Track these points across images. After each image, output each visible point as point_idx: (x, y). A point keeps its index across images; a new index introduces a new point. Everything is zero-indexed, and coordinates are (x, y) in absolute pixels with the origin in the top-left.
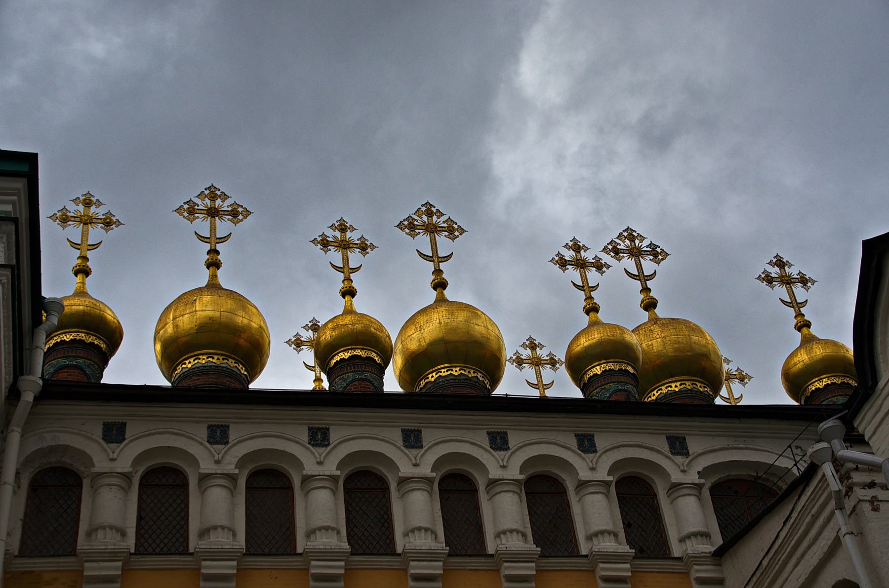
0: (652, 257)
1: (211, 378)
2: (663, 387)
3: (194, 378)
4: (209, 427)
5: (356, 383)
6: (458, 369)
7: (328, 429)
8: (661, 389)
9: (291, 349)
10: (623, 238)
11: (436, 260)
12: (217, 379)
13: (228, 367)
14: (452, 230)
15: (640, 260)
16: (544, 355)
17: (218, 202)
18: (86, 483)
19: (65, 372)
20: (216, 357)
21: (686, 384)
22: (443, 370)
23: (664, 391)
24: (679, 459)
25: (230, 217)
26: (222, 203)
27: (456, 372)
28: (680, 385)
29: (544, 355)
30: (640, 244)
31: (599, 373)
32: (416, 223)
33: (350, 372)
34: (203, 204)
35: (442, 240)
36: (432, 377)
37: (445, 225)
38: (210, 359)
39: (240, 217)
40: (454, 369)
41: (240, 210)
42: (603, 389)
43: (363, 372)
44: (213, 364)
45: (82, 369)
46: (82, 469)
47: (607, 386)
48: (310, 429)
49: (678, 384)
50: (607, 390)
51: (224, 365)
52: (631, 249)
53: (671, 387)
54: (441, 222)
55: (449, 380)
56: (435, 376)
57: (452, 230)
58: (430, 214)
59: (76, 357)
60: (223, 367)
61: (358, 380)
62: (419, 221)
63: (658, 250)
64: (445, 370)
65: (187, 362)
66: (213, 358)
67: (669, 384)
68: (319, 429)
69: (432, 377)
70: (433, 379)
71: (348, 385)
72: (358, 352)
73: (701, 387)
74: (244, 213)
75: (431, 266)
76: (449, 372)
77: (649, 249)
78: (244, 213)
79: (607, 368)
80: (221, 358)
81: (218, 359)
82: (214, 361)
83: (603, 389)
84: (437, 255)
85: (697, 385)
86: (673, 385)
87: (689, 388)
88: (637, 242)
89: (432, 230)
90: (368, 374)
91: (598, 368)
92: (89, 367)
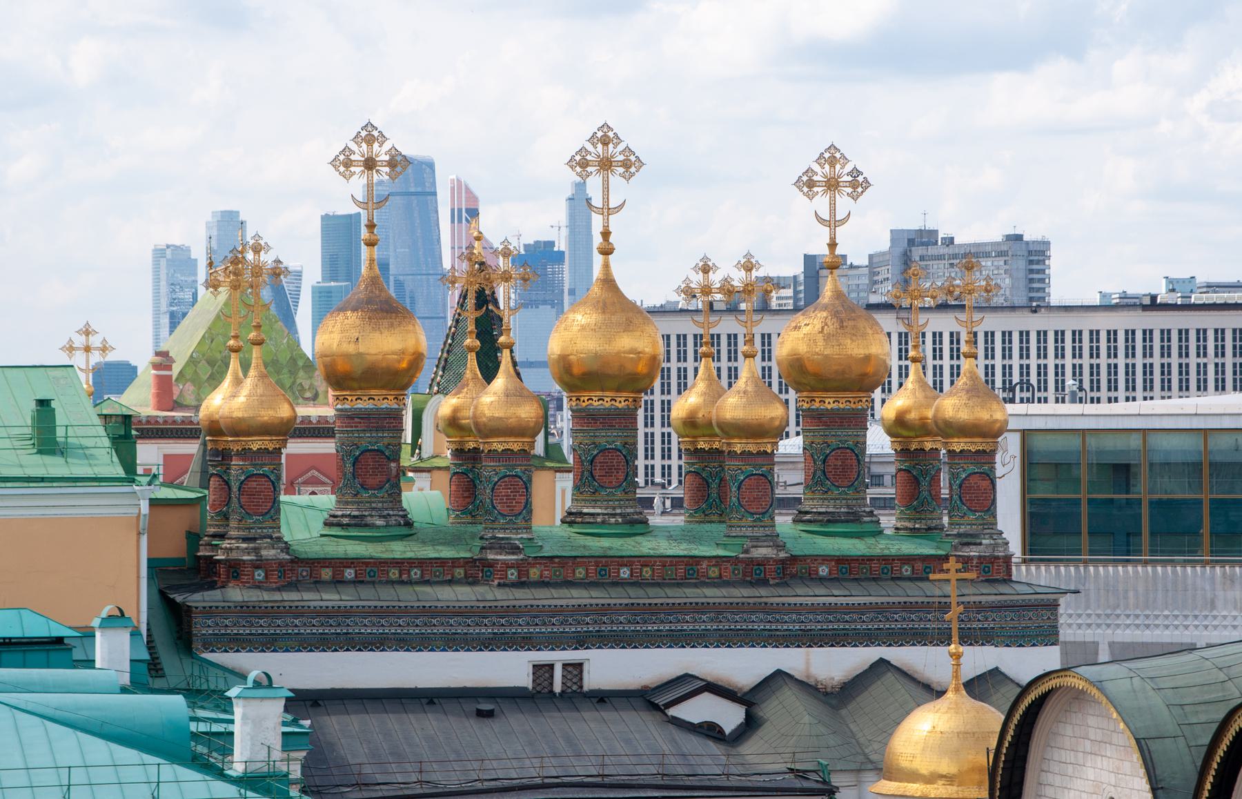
0: (849, 190)
1: (372, 423)
2: (817, 400)
3: (356, 420)
5: (506, 479)
6: (609, 399)
8: (814, 401)
10: (823, 161)
11: (606, 213)
14: (630, 165)
15: (835, 197)
16: (717, 281)
17: (376, 145)
19: (254, 481)
20: (376, 398)
22: (594, 399)
28: (834, 402)
29: (717, 281)
30: (841, 171)
31: (739, 452)
32: (589, 157)
33: (503, 466)
34: (359, 152)
35: (616, 180)
36: (584, 401)
37: (621, 158)
38: (371, 401)
40: (606, 399)
42: (740, 469)
43: (514, 467)
45: (268, 477)
47: (743, 468)
49: (831, 401)
51: (384, 406)
52: (829, 180)
53: (824, 402)
54: (617, 154)
55: (600, 409)
56: (587, 403)
58: (605, 141)
59: (262, 466)
61: (509, 476)
62: (593, 155)
63: (860, 179)
64: (596, 399)
65: (350, 398)
66: (374, 399)
69: (584, 401)
70: (584, 404)
71: (499, 480)
73: (854, 403)
76: (601, 402)
77: (850, 179)
79: (747, 450)
80: (381, 398)
83: (740, 469)
84: (608, 205)
85: (850, 402)
91: (739, 445)
92: (272, 472)
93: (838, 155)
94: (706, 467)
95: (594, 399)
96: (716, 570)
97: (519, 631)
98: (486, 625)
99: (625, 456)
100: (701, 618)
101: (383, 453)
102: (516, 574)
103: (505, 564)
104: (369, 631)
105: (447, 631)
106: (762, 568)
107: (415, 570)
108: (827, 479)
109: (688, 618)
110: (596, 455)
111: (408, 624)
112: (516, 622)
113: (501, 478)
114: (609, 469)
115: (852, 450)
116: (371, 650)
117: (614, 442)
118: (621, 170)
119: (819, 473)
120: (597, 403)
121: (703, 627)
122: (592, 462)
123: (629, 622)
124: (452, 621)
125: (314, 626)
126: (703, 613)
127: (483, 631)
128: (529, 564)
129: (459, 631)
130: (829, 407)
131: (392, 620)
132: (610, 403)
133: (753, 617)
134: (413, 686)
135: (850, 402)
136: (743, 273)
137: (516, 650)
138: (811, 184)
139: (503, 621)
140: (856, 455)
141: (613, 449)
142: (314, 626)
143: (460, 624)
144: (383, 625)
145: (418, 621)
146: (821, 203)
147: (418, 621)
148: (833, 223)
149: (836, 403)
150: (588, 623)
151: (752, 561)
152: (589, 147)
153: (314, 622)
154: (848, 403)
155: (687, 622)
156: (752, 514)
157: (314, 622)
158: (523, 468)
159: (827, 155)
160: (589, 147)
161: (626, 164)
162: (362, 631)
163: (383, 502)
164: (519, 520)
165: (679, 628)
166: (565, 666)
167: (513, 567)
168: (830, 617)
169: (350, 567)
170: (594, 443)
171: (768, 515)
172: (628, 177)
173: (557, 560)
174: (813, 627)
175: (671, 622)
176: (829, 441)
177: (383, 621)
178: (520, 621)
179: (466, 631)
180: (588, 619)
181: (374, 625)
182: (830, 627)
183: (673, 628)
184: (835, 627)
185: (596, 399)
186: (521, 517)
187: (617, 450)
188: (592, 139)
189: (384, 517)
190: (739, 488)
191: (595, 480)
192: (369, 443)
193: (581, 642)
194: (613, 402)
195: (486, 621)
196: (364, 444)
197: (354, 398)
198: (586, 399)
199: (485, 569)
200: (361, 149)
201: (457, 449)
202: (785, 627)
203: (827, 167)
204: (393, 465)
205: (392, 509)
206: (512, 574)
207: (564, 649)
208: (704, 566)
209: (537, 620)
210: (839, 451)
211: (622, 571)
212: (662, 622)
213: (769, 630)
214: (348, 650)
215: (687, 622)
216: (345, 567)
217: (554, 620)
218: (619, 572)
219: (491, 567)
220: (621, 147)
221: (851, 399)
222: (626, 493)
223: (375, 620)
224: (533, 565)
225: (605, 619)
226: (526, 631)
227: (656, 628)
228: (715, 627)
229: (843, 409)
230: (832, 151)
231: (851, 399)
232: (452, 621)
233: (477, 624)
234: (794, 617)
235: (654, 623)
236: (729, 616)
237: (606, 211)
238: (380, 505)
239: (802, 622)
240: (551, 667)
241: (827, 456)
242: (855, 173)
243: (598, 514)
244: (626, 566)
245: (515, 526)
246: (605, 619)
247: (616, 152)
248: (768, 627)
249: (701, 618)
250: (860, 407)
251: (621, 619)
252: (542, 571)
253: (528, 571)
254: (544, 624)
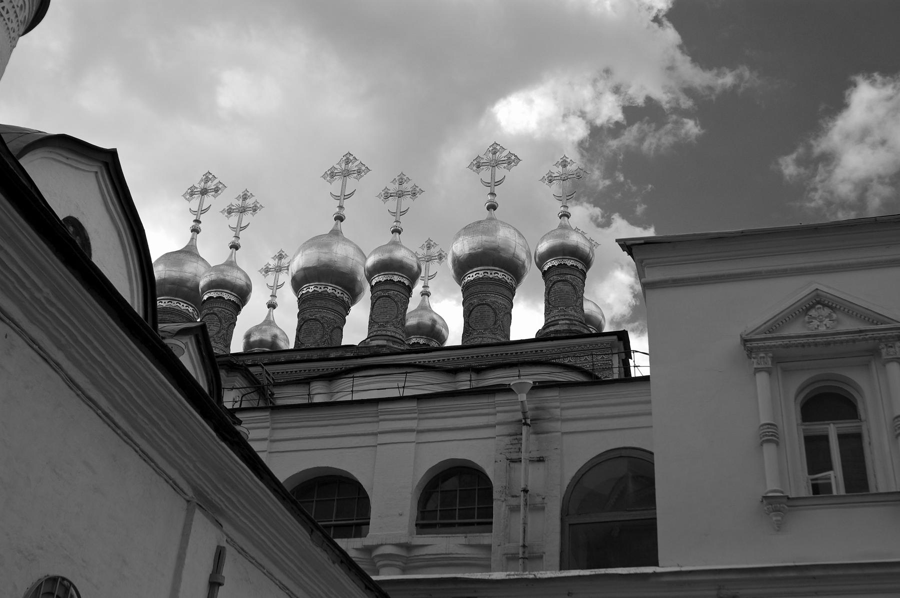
9: (261, 276)
12: (162, 316)
13: (172, 307)
44: (161, 307)
51: (168, 306)
60: (167, 308)
67: (477, 272)
81: (165, 303)
85: (488, 273)
90: (216, 309)
99: (321, 323)
108: (470, 327)
110: (303, 325)
114: (311, 332)
132: (313, 290)
135: (488, 273)
149: (478, 275)
154: (486, 274)
176: (472, 302)
187: (315, 320)
194: (316, 289)
230: (495, 146)
231: (488, 271)
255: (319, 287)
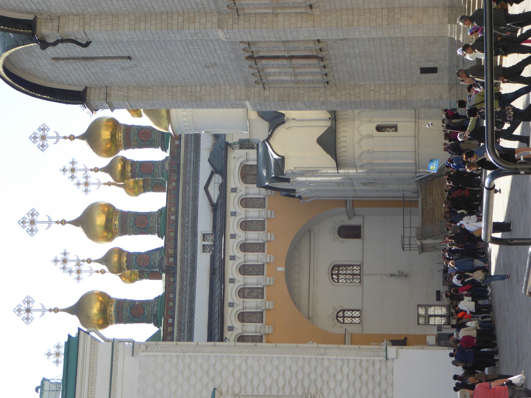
0: (46, 131)
3: (119, 317)
4: (229, 307)
5: (137, 262)
7: (230, 279)
11: (51, 222)
14: (33, 214)
17: (22, 308)
18: (242, 335)
21: (120, 136)
22: (115, 227)
23: (122, 144)
24: (238, 191)
25: (31, 304)
26: (23, 307)
27: (117, 223)
31: (131, 174)
34: (24, 314)
35: (38, 219)
37: (31, 216)
38: (112, 311)
39: (31, 300)
40: (115, 223)
41: (27, 300)
46: (239, 336)
48: (230, 283)
50: (139, 173)
56: (117, 230)
57: (33, 214)
63: (42, 127)
64: (115, 226)
68: (230, 281)
72: (125, 260)
74: (28, 298)
75: (54, 225)
76: (116, 225)
78: (28, 298)
82: (112, 310)
85: (121, 132)
86: (120, 140)
87: (122, 135)
88: (37, 136)
89: (32, 222)
93: (33, 136)
94: (149, 184)
95: (115, 227)
96: (173, 183)
97: (190, 257)
98: (187, 270)
100: (188, 189)
101: (131, 307)
102: (171, 258)
103: (167, 263)
104: (187, 314)
105: (189, 285)
106: (173, 166)
107: (170, 296)
109: (188, 194)
111: (185, 299)
112: (186, 259)
113: (137, 264)
115: (139, 131)
116: (194, 313)
117: (132, 220)
118: (35, 216)
119: (147, 143)
120: (117, 226)
121: (191, 189)
122: (139, 228)
123: (188, 216)
124: (185, 283)
125: (184, 335)
126: (186, 188)
127: (189, 271)
128: (167, 254)
129: (189, 280)
130: (122, 139)
131: (183, 305)
132: (117, 222)
133: (189, 170)
134: (208, 298)
135: (121, 132)
136: (67, 172)
137: (196, 259)
138: (43, 146)
139: (186, 264)
140: (141, 129)
141: (134, 221)
142: (184, 335)
143: (186, 280)
144: (185, 309)
145: (184, 296)
146: (50, 142)
147: (184, 296)
148: (58, 138)
149: (121, 137)
150: (188, 232)
151: (170, 170)
152: (26, 228)
153: (183, 335)
155: (189, 194)
156: (154, 169)
157: (183, 335)
158: (133, 255)
159: (33, 140)
160: (26, 228)
161: (33, 215)
162: (187, 316)
163: (149, 307)
164: (152, 257)
165: (191, 198)
166: (204, 240)
167: (169, 260)
168: (190, 141)
169: (168, 321)
170: (132, 228)
171: (155, 164)
172: (37, 214)
173: (167, 243)
174: (193, 147)
175: (189, 201)
177: (184, 309)
178: (186, 257)
179: (189, 278)
180: (186, 232)
181: (185, 312)
182: (193, 141)
183: (191, 200)
184: (193, 139)
185: (115, 226)
186: (151, 256)
188: (24, 227)
189: (154, 307)
190: (145, 174)
191: (146, 227)
192: (127, 312)
193: (195, 234)
194: (117, 221)
195: (185, 270)
196: (128, 314)
197: (111, 317)
198: (116, 231)
199: (170, 270)
200: (23, 314)
201: (139, 278)
202: (193, 158)
203: (37, 140)
204: (137, 303)
205: (152, 303)
206: (171, 260)
207: (197, 241)
208: (171, 188)
209: (186, 251)
210: (139, 136)
211: (172, 219)
212: (189, 204)
213: (193, 164)
214: (194, 322)
215: (189, 194)
216: (168, 322)
217: (186, 245)
218: (172, 220)
219: (169, 267)
220: (27, 216)
221: (120, 131)
222: (151, 216)
223: (183, 312)
224: (168, 252)
225: (187, 225)
226: (190, 255)
227: (191, 206)
228: (192, 184)
229: (123, 134)
231: (120, 131)
232: (185, 283)
233: (187, 273)
234: (189, 154)
235: (189, 207)
236: (188, 179)
237: (50, 222)
238: (150, 308)
239: (191, 151)
240: (204, 246)
241: (141, 140)
242: (40, 129)
243: (158, 226)
244: (170, 217)
245: (154, 258)
246: (187, 225)
247: (29, 219)
248: (192, 164)
249: (188, 189)
250: (123, 128)
251: (187, 219)
252: (171, 249)
253: (170, 254)
254: (187, 248)
255: (116, 219)
